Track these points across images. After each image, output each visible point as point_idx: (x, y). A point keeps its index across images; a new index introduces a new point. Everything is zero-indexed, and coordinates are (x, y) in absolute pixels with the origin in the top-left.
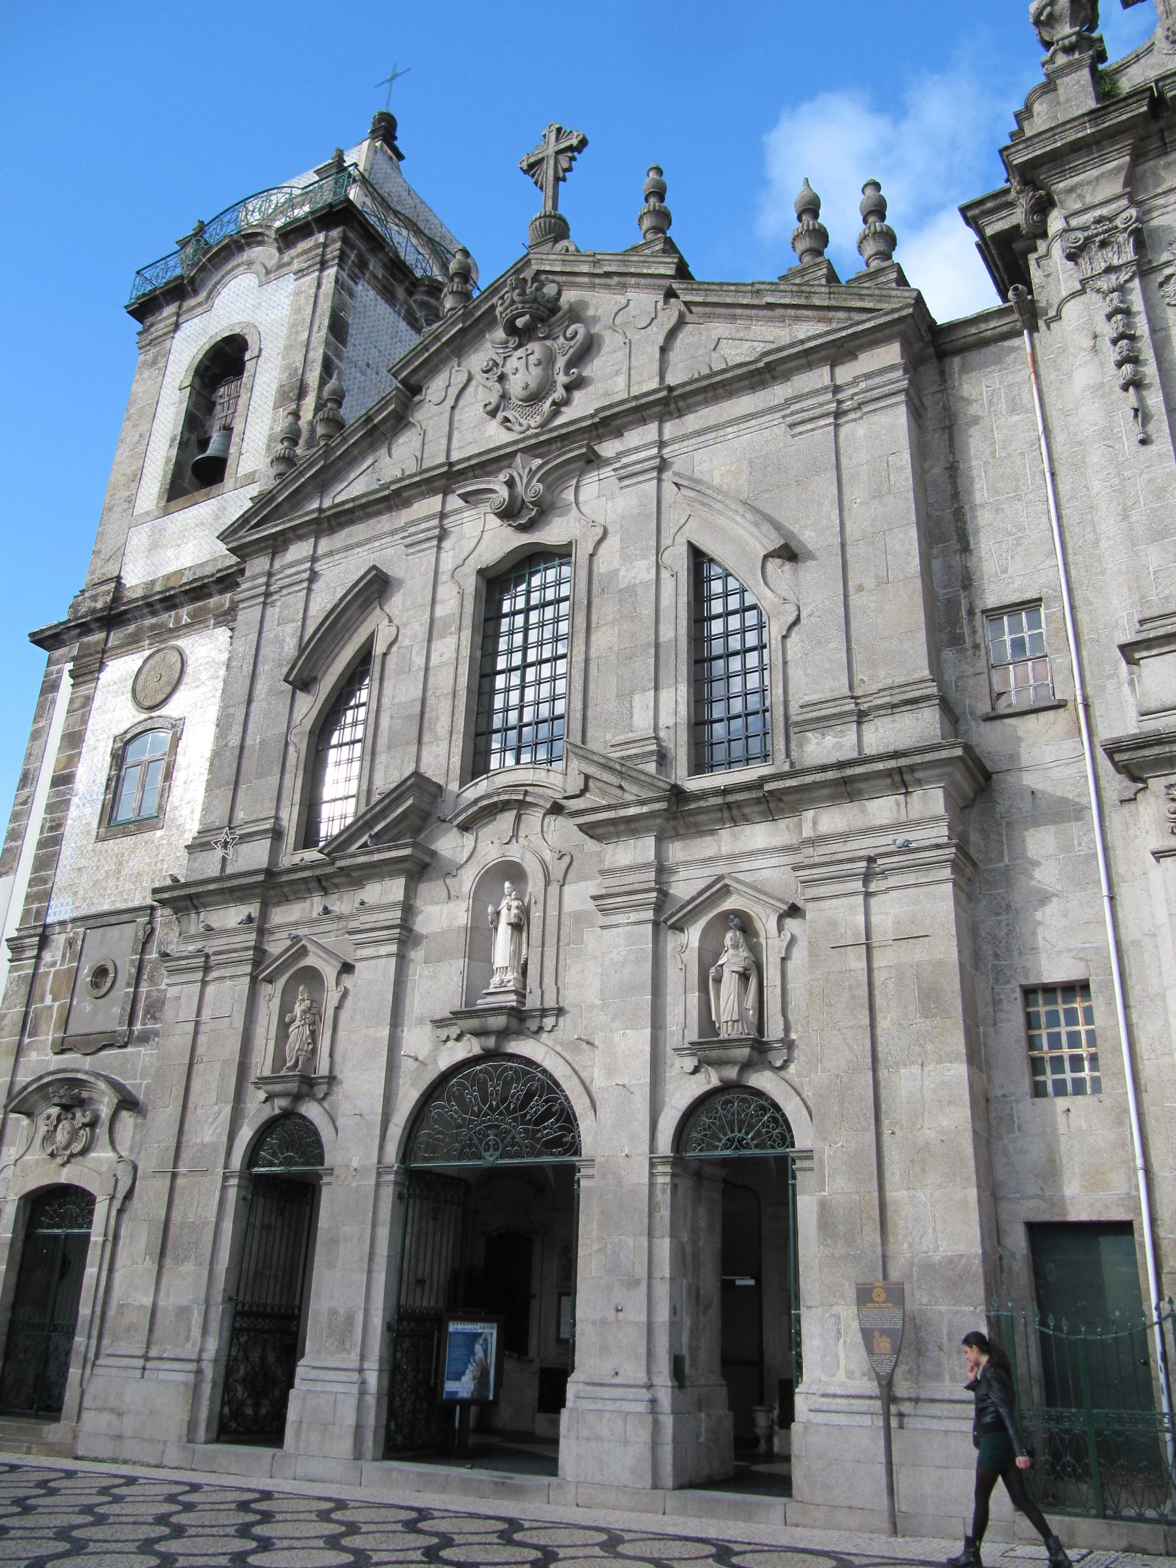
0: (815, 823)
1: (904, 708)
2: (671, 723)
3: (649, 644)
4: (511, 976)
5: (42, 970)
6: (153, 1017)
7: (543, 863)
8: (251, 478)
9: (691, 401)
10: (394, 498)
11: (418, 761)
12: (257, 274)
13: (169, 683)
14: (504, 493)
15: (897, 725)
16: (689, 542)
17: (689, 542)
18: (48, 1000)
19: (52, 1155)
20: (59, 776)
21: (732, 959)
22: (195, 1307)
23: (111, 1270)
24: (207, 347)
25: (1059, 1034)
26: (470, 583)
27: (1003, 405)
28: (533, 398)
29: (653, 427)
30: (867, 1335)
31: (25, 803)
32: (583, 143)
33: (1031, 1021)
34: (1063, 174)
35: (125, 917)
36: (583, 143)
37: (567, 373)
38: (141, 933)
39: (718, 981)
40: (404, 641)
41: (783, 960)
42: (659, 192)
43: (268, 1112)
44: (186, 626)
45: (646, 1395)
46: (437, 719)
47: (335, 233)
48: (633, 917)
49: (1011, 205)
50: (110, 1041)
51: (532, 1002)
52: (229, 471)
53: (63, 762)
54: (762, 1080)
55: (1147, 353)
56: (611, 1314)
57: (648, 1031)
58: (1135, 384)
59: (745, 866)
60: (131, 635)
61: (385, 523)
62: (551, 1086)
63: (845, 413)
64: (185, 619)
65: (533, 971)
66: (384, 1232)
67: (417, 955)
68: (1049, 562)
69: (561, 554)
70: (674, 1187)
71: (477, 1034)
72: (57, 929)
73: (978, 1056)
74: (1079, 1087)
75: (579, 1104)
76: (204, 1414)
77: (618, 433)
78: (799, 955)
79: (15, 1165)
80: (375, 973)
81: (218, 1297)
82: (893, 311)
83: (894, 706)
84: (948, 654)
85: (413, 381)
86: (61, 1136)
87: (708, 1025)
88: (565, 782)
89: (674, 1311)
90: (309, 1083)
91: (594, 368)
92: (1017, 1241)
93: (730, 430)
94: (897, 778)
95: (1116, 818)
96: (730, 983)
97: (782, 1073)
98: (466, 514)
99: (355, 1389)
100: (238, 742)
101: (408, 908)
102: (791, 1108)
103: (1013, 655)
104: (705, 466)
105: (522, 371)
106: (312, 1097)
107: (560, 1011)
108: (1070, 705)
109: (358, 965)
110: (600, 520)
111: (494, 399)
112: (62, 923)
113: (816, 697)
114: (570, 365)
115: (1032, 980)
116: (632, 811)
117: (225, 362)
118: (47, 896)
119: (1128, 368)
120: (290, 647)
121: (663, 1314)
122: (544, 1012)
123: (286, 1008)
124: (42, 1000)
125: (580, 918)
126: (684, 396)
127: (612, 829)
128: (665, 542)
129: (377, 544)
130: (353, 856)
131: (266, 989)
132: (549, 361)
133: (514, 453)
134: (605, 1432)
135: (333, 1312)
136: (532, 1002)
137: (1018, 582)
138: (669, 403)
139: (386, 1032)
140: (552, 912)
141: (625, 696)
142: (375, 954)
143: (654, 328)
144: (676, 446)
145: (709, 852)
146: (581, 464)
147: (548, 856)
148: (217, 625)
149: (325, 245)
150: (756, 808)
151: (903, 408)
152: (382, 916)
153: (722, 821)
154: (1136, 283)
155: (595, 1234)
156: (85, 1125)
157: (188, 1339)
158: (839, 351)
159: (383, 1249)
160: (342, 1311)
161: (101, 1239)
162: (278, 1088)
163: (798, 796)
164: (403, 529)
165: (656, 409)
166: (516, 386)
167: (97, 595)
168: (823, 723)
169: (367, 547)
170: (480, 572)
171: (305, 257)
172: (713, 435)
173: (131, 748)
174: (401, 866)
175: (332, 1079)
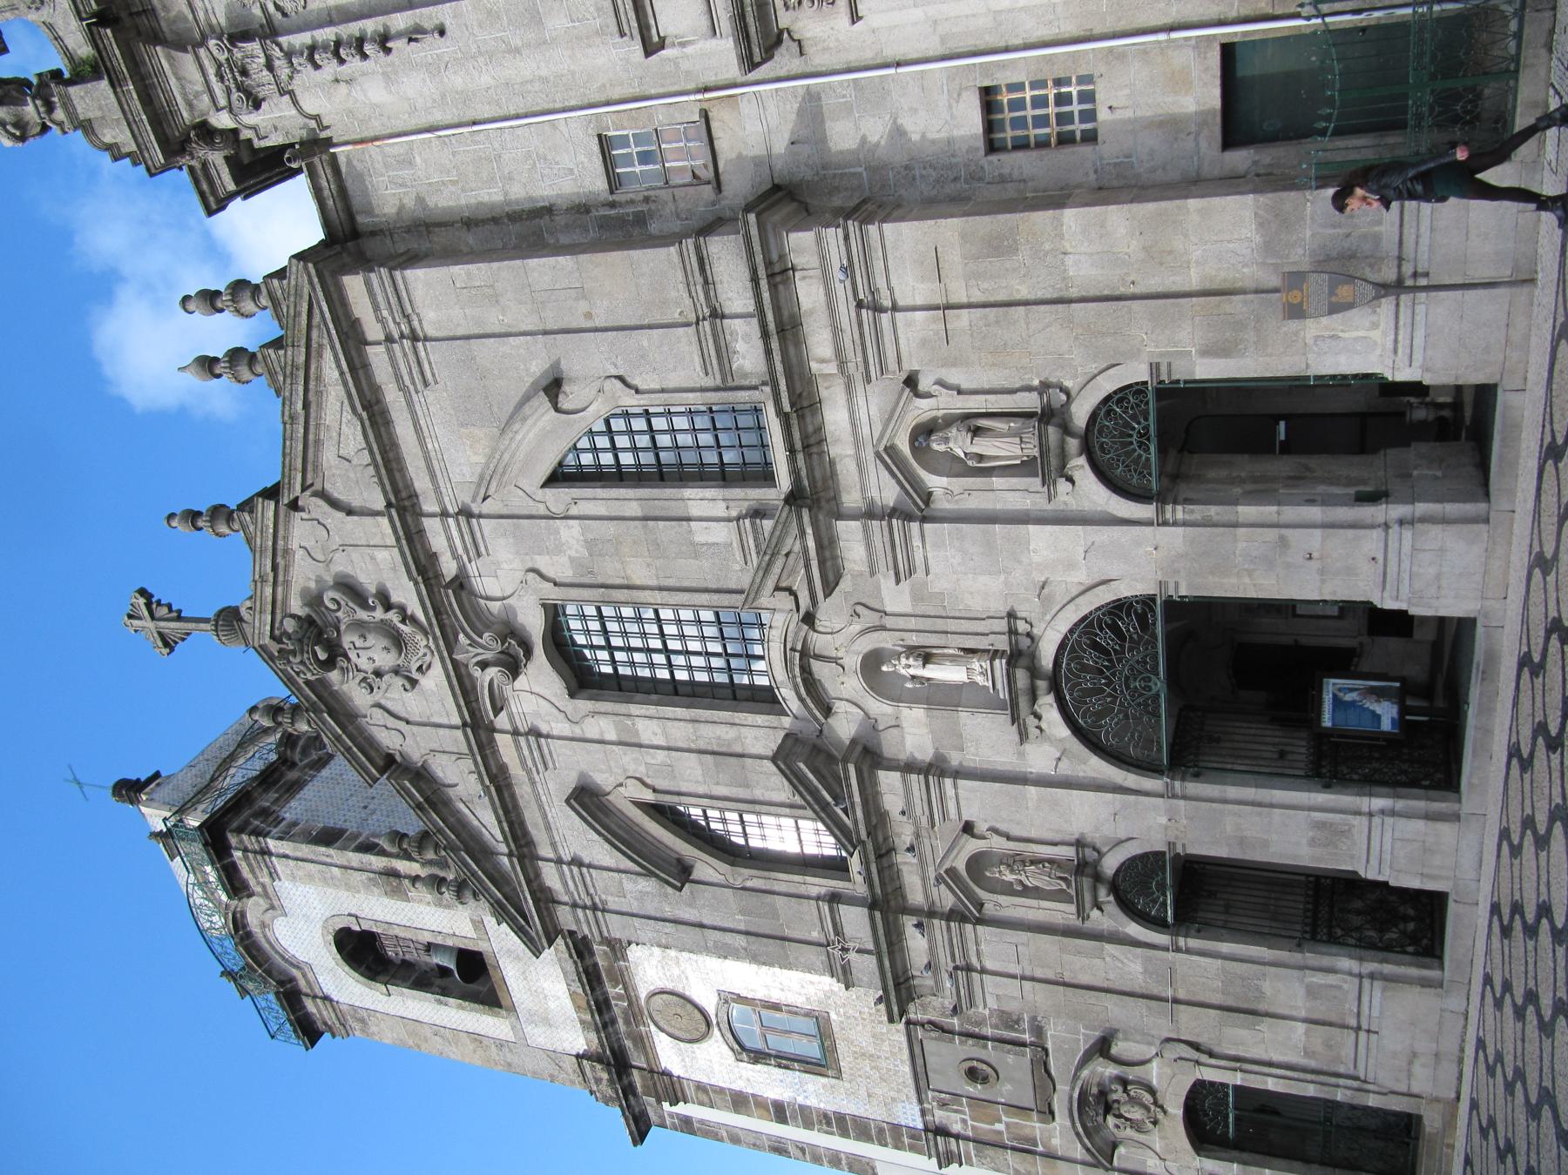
0: (823, 361)
2: (723, 505)
3: (645, 527)
4: (976, 665)
5: (970, 1133)
6: (1017, 1022)
7: (864, 632)
8: (478, 925)
9: (401, 485)
10: (498, 781)
11: (761, 757)
12: (274, 918)
13: (683, 1007)
14: (493, 672)
15: (726, 278)
16: (543, 486)
17: (543, 486)
18: (1000, 1127)
19: (1155, 1123)
21: (959, 443)
22: (1308, 980)
23: (1270, 1064)
24: (347, 968)
25: (1034, 117)
26: (583, 705)
27: (405, 173)
28: (398, 642)
29: (428, 523)
30: (1335, 309)
31: (803, 1150)
32: (143, 592)
33: (1021, 145)
34: (174, 113)
35: (917, 1050)
36: (143, 592)
37: (373, 609)
38: (933, 1034)
39: (981, 458)
40: (641, 771)
41: (960, 392)
42: (192, 516)
43: (1111, 907)
44: (626, 989)
45: (1394, 530)
47: (233, 840)
48: (917, 542)
49: (205, 165)
50: (1041, 1065)
51: (1002, 643)
52: (471, 946)
54: (1080, 413)
55: (354, 28)
56: (1315, 565)
57: (1031, 527)
58: (384, 41)
59: (866, 430)
61: (523, 791)
62: (1086, 625)
63: (413, 330)
64: (619, 990)
65: (971, 643)
66: (1233, 792)
67: (955, 759)
68: (562, 127)
69: (554, 616)
70: (1187, 501)
71: (1034, 698)
72: (929, 1118)
73: (1056, 198)
74: (1087, 97)
75: (1105, 596)
76: (1414, 972)
77: (433, 557)
78: (955, 377)
80: (973, 800)
81: (1297, 957)
82: (311, 282)
83: (706, 282)
84: (654, 227)
85: (381, 763)
86: (1136, 1114)
87: (1025, 468)
88: (781, 611)
89: (1311, 502)
90: (1083, 867)
91: (369, 583)
92: (1241, 158)
93: (430, 446)
94: (778, 279)
95: (818, 60)
96: (983, 446)
97: (1073, 393)
98: (514, 710)
99: (1389, 821)
100: (742, 937)
101: (909, 767)
102: (1108, 384)
103: (655, 163)
104: (466, 470)
105: (371, 653)
106: (1097, 863)
107: (1011, 615)
108: (705, 106)
109: (965, 818)
110: (520, 575)
111: (399, 681)
112: (923, 1113)
113: (697, 360)
114: (365, 605)
115: (980, 144)
116: (811, 543)
117: (362, 950)
118: (896, 1129)
119: (368, 48)
120: (647, 885)
121: (1314, 513)
122: (1012, 632)
123: (1008, 889)
124: (999, 1133)
125: (917, 597)
126: (396, 492)
127: (829, 564)
128: (542, 510)
130: (856, 822)
131: (989, 909)
132: (361, 627)
133: (453, 661)
134: (1432, 571)
135: (1312, 842)
136: (1002, 643)
137: (582, 158)
138: (404, 507)
139: (1032, 789)
140: (912, 623)
141: (696, 550)
143: (328, 522)
144: (446, 499)
145: (853, 467)
146: (464, 595)
147: (856, 628)
148: (625, 958)
149: (245, 850)
150: (808, 420)
151: (408, 273)
153: (821, 453)
154: (283, 40)
155: (1234, 580)
156: (1125, 1090)
157: (1339, 988)
158: (351, 337)
159: (1249, 793)
161: (1239, 1075)
162: (1088, 897)
163: (796, 377)
164: (529, 772)
165: (409, 519)
166: (386, 659)
168: (723, 353)
170: (572, 695)
172: (435, 463)
173: (748, 1044)
174: (866, 775)
175: (1079, 844)
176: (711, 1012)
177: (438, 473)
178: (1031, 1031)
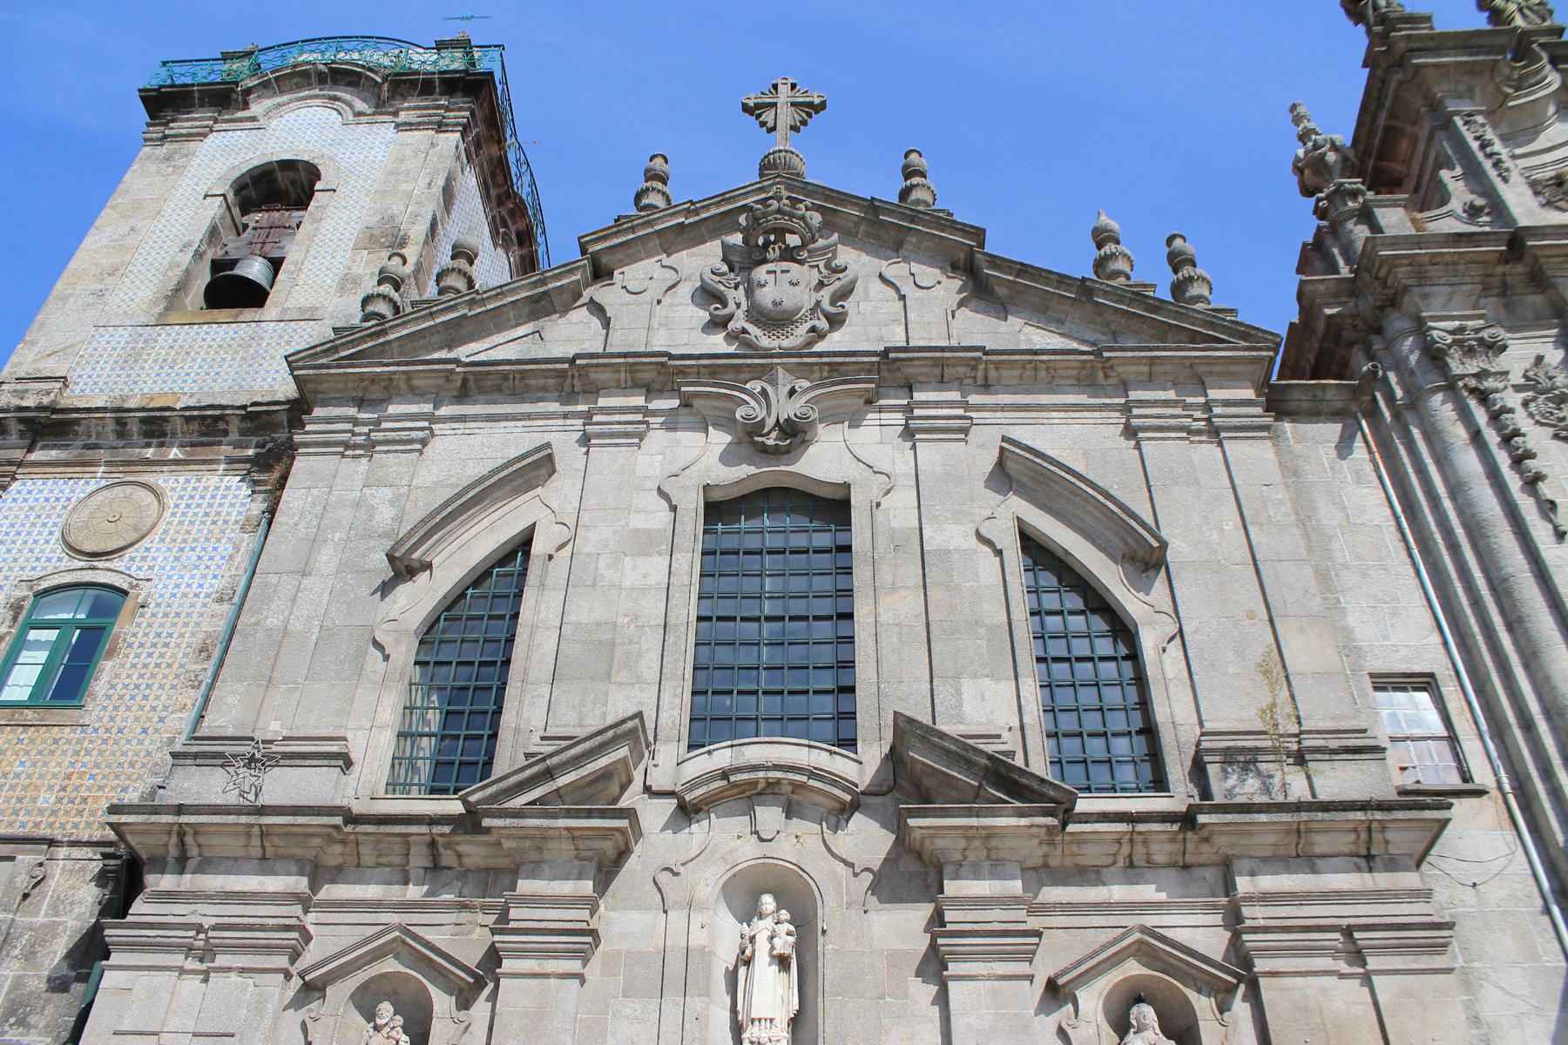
1: (1345, 756)
10: (572, 380)
24: (256, 163)
32: (823, 106)
36: (823, 106)
83: (1334, 752)
88: (861, 773)
93: (1055, 414)
117: (280, 189)
130: (518, 814)
137: (1403, 653)
142: (537, 970)
144: (987, 415)
170: (706, 487)
172: (1034, 414)
176: (116, 564)
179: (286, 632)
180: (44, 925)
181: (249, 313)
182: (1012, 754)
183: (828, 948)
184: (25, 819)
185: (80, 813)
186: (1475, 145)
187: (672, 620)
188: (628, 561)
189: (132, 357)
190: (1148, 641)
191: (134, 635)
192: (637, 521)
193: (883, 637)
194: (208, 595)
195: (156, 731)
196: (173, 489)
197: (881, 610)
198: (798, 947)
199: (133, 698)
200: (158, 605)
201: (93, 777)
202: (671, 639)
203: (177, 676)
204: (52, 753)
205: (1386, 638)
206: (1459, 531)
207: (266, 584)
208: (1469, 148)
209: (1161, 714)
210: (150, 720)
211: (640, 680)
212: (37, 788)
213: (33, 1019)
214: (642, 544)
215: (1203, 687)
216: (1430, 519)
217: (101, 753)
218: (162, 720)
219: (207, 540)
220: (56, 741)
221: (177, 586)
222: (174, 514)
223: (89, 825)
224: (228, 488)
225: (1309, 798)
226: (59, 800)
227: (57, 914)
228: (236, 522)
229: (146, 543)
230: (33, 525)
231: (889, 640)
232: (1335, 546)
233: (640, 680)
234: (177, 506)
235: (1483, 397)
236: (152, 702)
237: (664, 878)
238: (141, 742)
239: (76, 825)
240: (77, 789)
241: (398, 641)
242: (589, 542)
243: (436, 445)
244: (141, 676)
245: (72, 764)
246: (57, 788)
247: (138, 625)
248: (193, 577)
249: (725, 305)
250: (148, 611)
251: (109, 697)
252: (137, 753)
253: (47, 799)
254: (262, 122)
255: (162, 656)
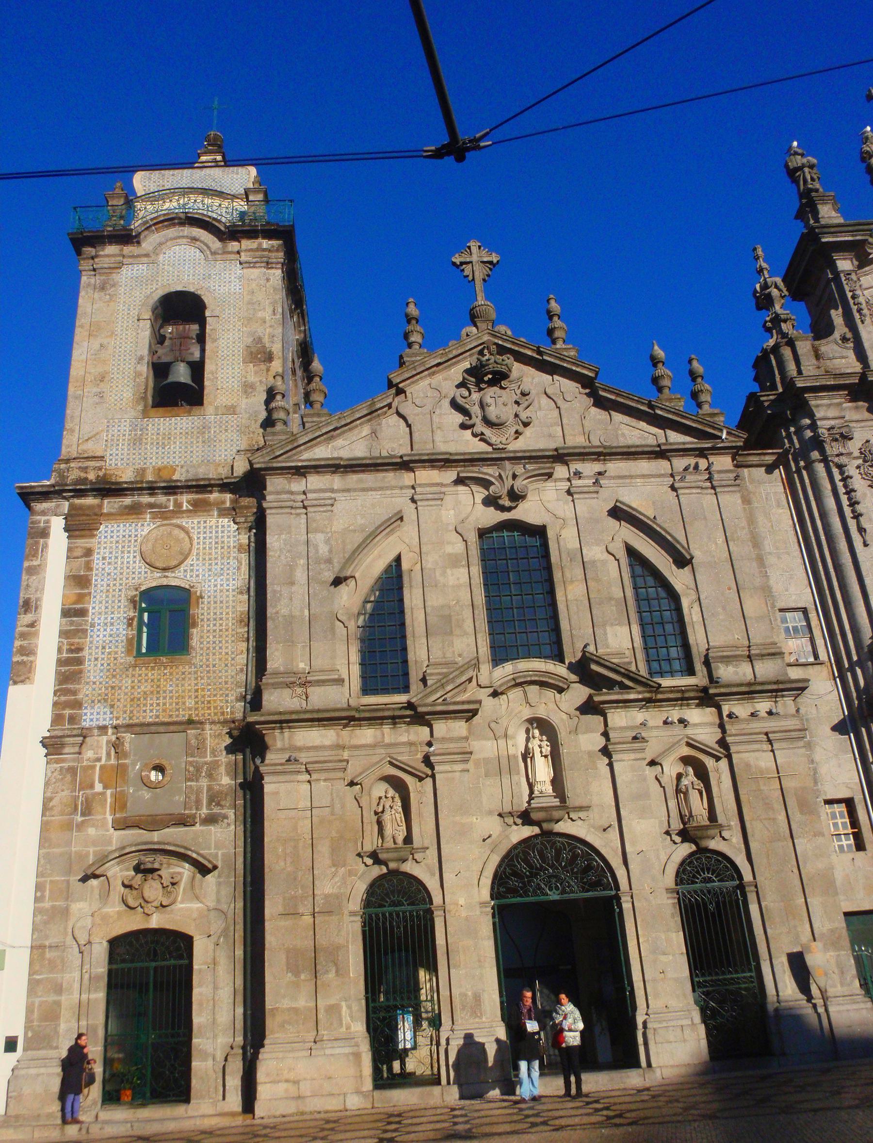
6: (218, 804)
7: (562, 719)
16: (626, 543)
18: (98, 787)
20: (70, 609)
44: (188, 511)
46: (463, 620)
53: (73, 598)
60: (126, 507)
72: (96, 732)
79: (92, 915)
83: (763, 655)
93: (638, 480)
112: (103, 729)
118: (78, 705)
122: (581, 808)
124: (92, 786)
129: (389, 492)
134: (672, 1039)
148: (221, 515)
152: (452, 745)
157: (341, 1024)
160: (470, 993)
167: (87, 468)
169: (380, 492)
171: (252, 253)
177: (621, 481)
178: (209, 814)
179: (292, 617)
180: (211, 762)
181: (196, 410)
182: (630, 663)
183: (564, 751)
184: (183, 713)
185: (209, 708)
186: (849, 295)
187: (475, 603)
188: (449, 571)
189: (137, 441)
190: (685, 603)
191: (202, 614)
192: (449, 549)
193: (570, 606)
194: (233, 590)
195: (232, 665)
196: (193, 528)
197: (568, 592)
198: (551, 752)
199: (214, 648)
200: (209, 597)
201: (209, 690)
202: (476, 612)
203: (233, 636)
204: (184, 679)
205: (787, 590)
206: (823, 538)
207: (275, 591)
208: (846, 295)
209: (691, 640)
210: (227, 659)
211: (466, 634)
212: (183, 697)
213: (223, 803)
214: (453, 561)
215: (709, 627)
216: (810, 529)
217: (209, 678)
218: (233, 659)
219: (222, 558)
220: (183, 673)
221: (215, 586)
222: (198, 543)
223: (215, 714)
224: (223, 526)
225: (753, 681)
226: (197, 703)
227: (215, 756)
228: (234, 547)
229: (189, 561)
230: (123, 552)
231: (573, 608)
232: (766, 542)
233: (466, 634)
234: (198, 538)
235: (840, 467)
236: (224, 651)
237: (493, 725)
238: (226, 671)
239: (209, 714)
240: (203, 696)
241: (349, 619)
242: (430, 561)
243: (338, 507)
244: (214, 637)
245: (196, 684)
246: (193, 697)
247: (203, 609)
248: (222, 580)
249: (470, 418)
250: (206, 600)
251: (202, 649)
252: (226, 677)
253: (190, 703)
254: (153, 257)
255: (221, 625)
